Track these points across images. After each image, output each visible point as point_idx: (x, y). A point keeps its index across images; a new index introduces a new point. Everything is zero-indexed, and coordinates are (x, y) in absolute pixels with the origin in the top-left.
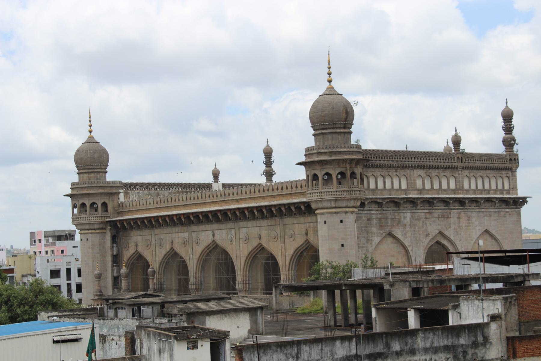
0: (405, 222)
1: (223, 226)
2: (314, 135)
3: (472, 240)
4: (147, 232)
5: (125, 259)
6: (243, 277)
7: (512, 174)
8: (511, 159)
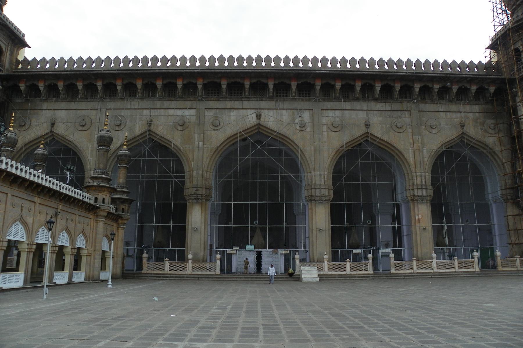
1: (286, 105)
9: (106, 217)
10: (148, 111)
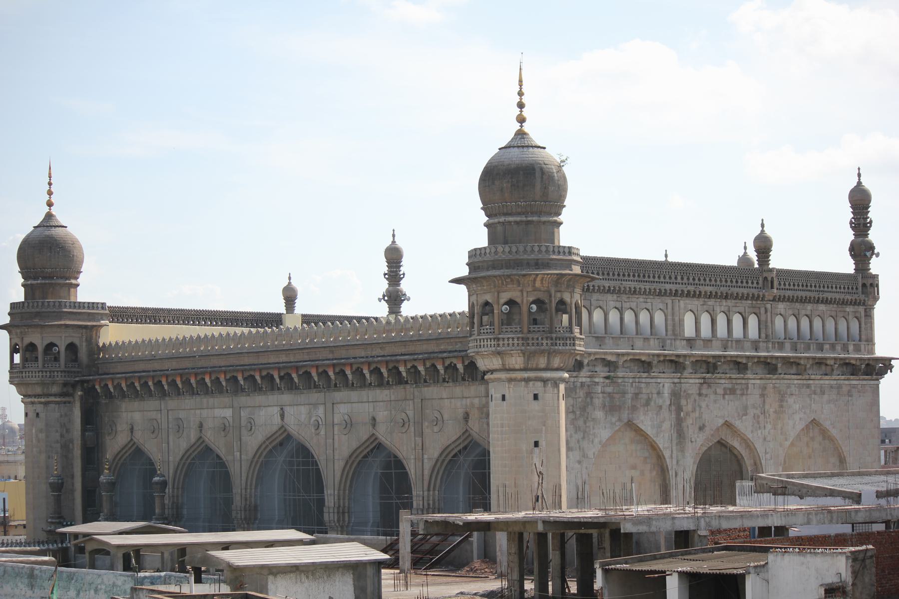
0: (660, 402)
1: (302, 398)
2: (485, 225)
3: (786, 440)
4: (153, 404)
5: (109, 456)
6: (339, 499)
7: (866, 316)
8: (864, 285)
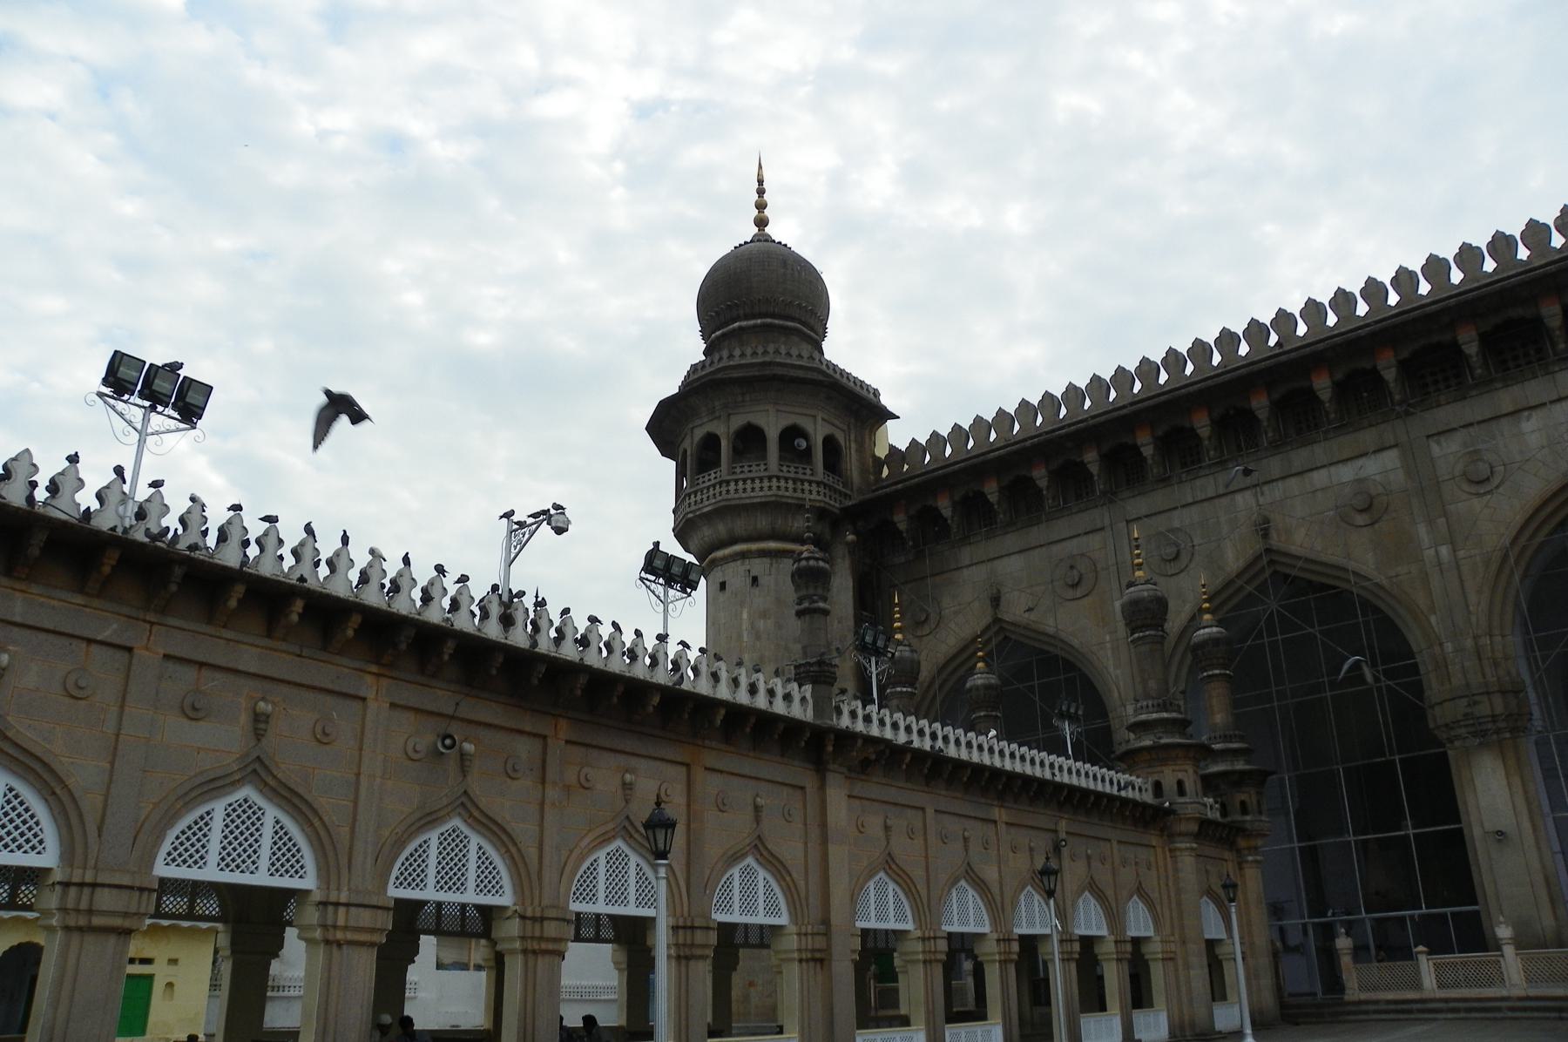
9: (1197, 836)
10: (1248, 494)
